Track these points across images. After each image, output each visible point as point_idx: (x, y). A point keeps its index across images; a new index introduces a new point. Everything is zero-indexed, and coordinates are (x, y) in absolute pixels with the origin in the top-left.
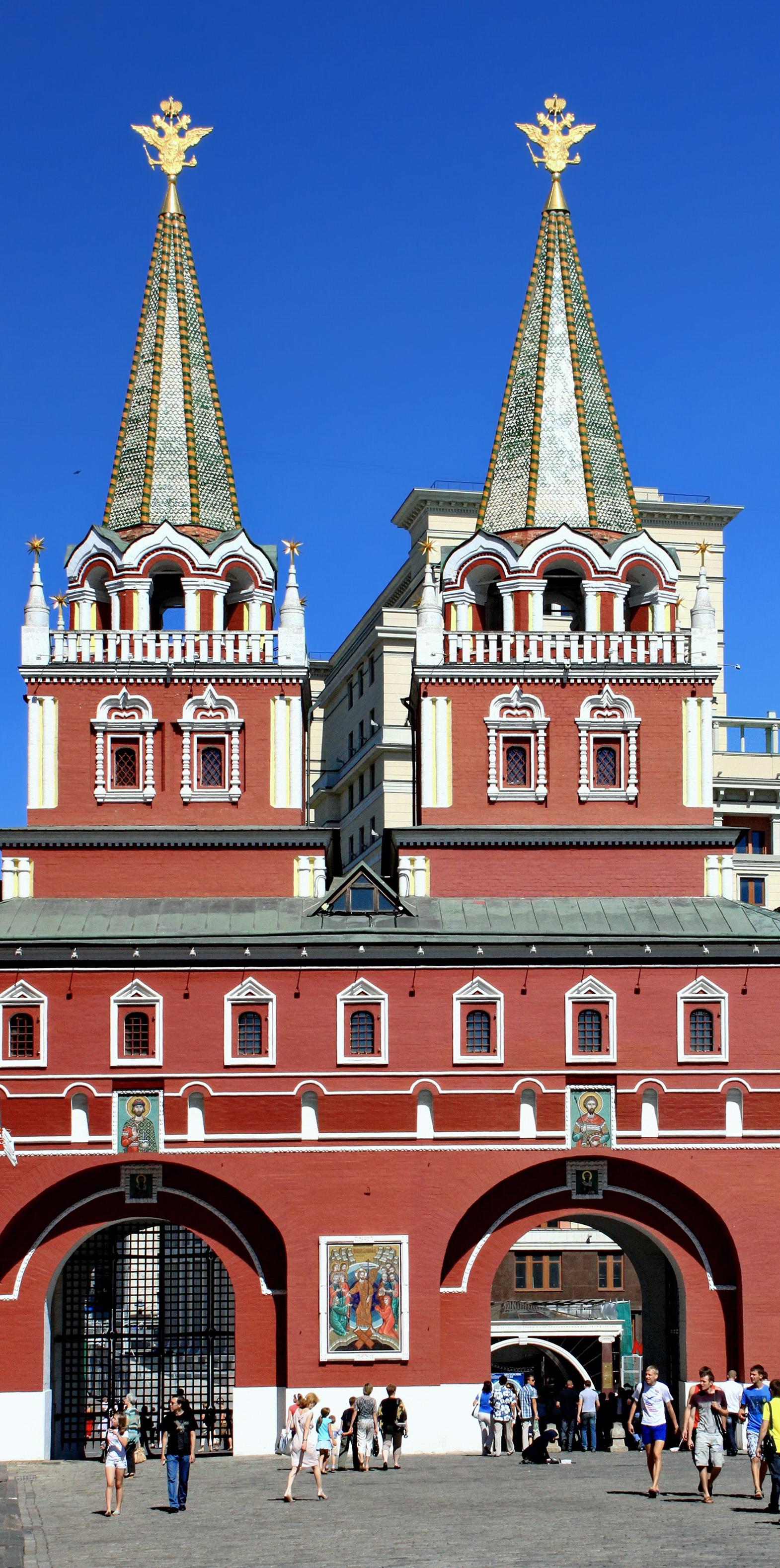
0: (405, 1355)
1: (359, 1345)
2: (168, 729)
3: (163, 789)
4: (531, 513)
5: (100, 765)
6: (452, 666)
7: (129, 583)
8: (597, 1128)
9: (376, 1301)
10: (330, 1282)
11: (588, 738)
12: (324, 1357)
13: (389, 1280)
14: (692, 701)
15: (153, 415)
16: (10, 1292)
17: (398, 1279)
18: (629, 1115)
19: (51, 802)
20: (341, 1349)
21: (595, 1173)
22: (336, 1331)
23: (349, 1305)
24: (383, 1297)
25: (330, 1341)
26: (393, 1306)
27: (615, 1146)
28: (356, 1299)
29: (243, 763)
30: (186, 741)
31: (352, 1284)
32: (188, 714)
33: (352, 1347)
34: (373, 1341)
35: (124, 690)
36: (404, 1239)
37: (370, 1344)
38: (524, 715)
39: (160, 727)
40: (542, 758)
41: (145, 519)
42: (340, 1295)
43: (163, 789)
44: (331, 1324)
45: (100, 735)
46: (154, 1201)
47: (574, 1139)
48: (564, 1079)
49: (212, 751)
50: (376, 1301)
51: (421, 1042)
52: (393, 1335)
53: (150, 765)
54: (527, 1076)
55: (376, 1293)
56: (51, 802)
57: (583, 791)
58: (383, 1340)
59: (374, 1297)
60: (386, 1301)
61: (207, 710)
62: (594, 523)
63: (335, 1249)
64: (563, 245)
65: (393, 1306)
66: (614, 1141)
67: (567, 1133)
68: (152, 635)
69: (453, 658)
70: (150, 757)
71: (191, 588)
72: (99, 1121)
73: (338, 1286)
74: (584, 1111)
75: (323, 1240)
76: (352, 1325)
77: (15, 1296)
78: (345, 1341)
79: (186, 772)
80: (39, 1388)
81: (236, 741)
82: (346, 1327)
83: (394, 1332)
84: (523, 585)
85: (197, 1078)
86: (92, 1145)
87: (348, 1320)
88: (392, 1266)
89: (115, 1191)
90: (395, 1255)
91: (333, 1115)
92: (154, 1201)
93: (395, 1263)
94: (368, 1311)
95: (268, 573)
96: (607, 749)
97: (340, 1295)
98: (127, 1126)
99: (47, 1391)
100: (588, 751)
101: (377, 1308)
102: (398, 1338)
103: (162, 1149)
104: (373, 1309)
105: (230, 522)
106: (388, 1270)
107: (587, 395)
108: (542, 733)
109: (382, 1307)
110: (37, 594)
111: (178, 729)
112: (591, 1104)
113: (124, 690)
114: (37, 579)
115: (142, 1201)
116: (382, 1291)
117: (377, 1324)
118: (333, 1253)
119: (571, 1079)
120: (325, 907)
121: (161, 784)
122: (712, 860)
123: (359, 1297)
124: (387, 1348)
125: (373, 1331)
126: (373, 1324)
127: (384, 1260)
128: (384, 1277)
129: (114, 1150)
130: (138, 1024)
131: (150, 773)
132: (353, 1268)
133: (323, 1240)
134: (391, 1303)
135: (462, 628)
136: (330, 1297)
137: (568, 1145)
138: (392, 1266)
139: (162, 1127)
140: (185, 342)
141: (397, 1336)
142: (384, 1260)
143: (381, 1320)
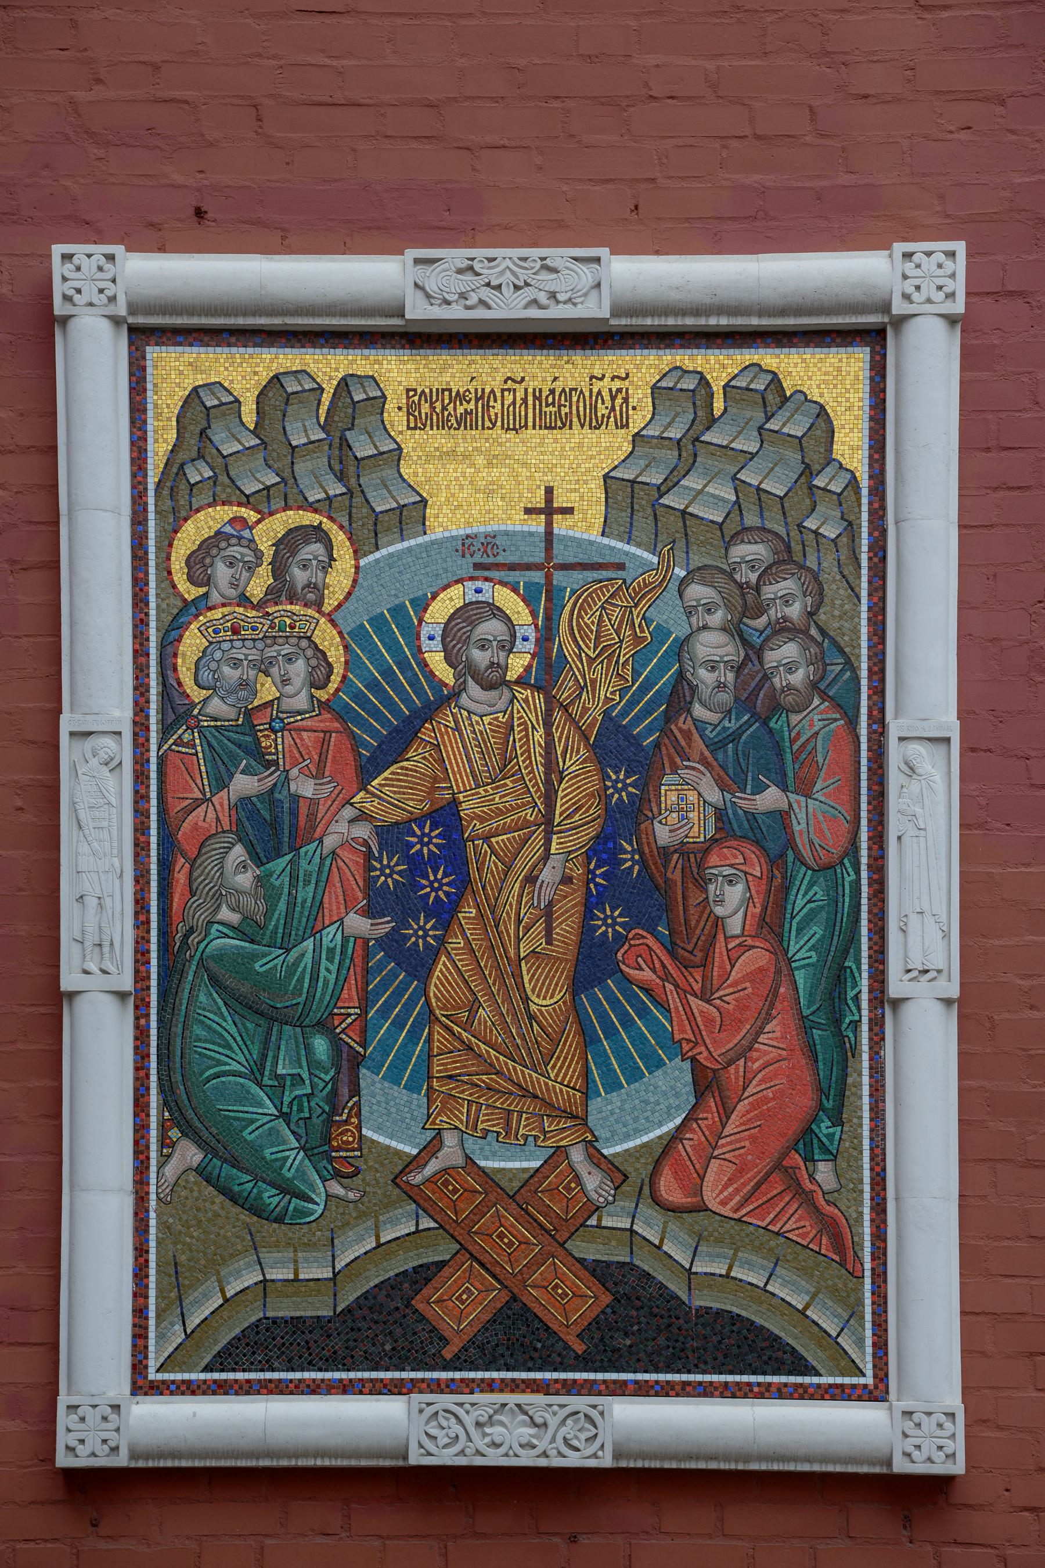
1: (460, 1307)
9: (637, 891)
12: (114, 1406)
13: (756, 696)
17: (855, 685)
20: (273, 1348)
23: (358, 924)
24: (694, 859)
26: (803, 948)
31: (389, 721)
34: (600, 1272)
37: (570, 1304)
42: (273, 829)
52: (797, 1224)
55: (623, 820)
58: (685, 1259)
59: (602, 848)
60: (732, 901)
65: (803, 948)
73: (245, 739)
76: (389, 1123)
82: (328, 1134)
83: (806, 1199)
87: (350, 1063)
88: (786, 558)
97: (273, 829)
101: (643, 963)
104: (592, 964)
106: (746, 602)
109: (693, 945)
116: (685, 805)
118: (202, 411)
123: (455, 856)
125: (593, 1181)
126: (601, 1110)
128: (713, 645)
133: (99, 280)
134: (771, 922)
138: (786, 558)
141: (837, 1237)
142: (707, 495)
143: (674, 1080)
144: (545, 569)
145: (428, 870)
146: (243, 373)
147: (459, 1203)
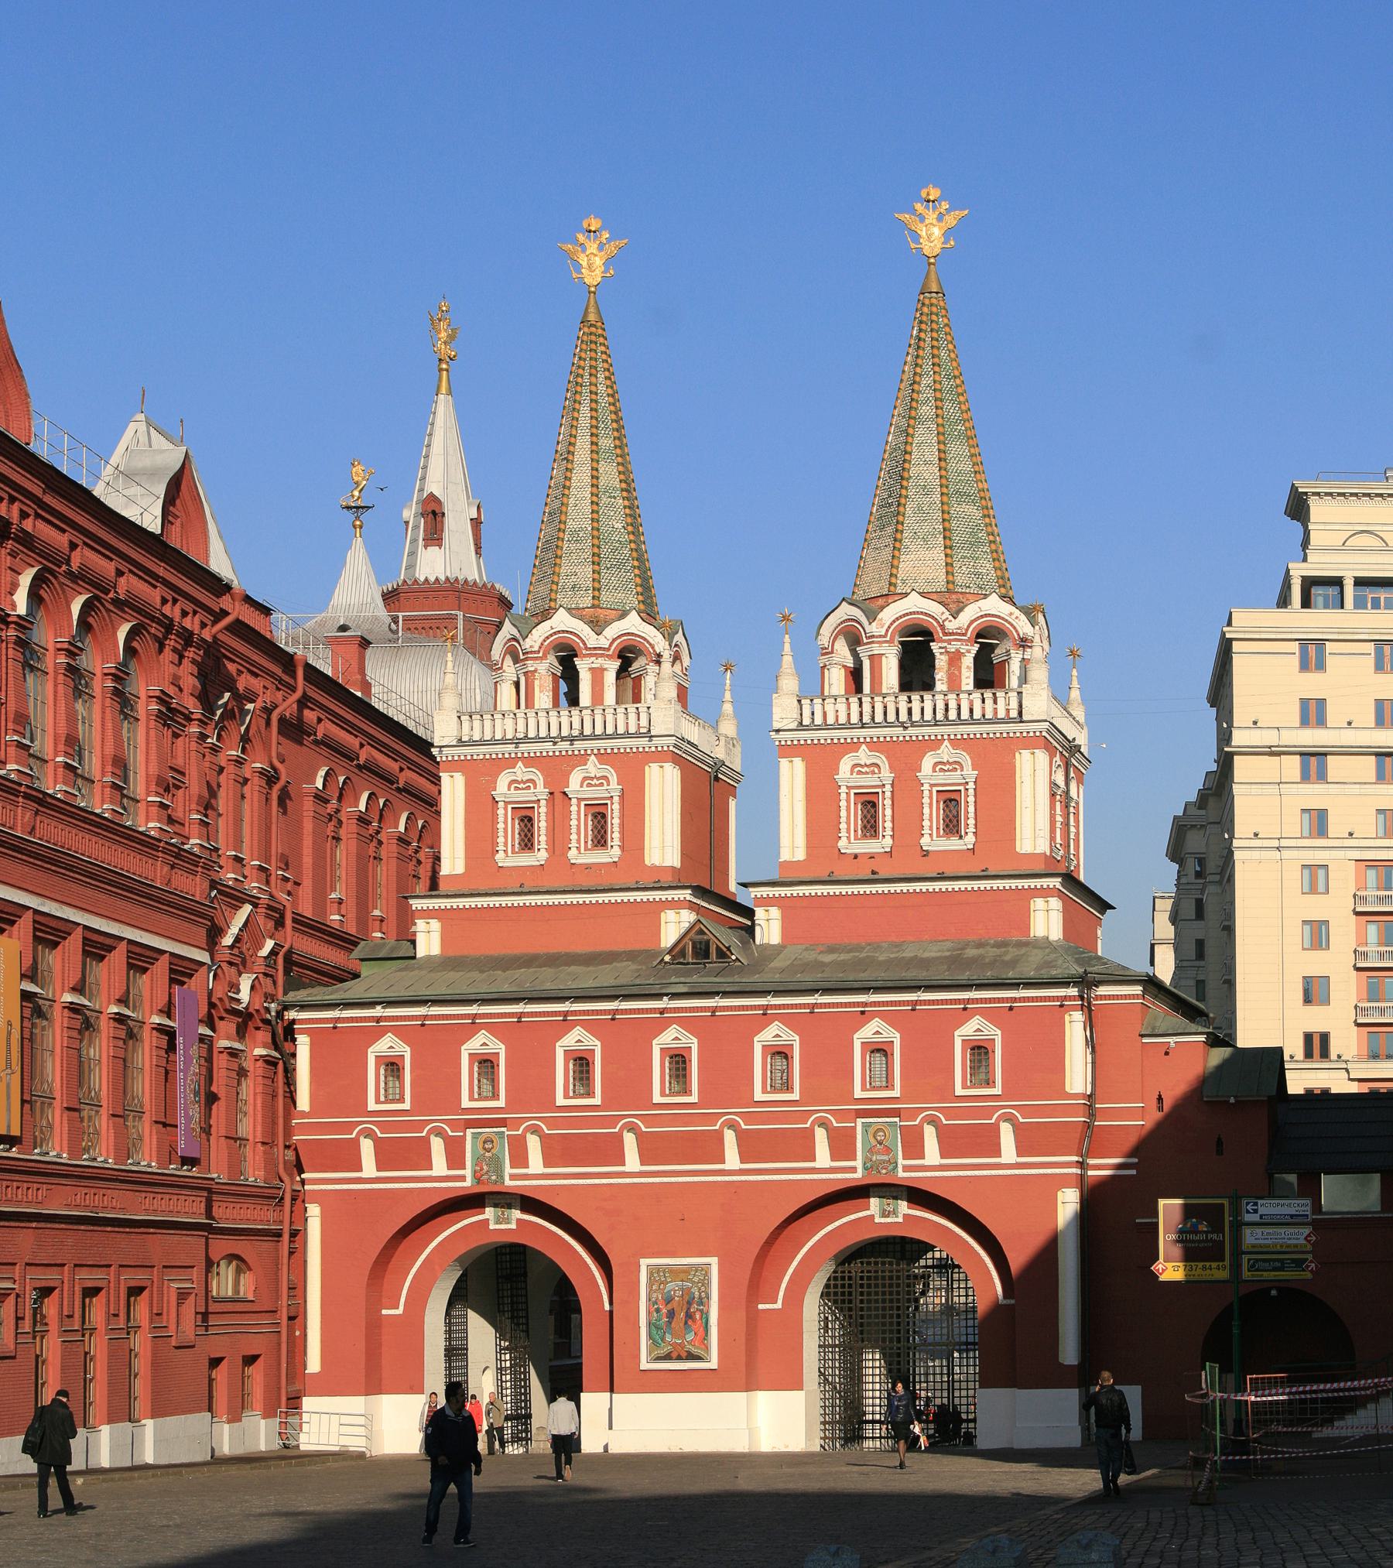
0: (713, 1364)
1: (674, 1355)
2: (558, 796)
4: (893, 580)
5: (501, 833)
6: (807, 728)
7: (531, 666)
8: (886, 1158)
9: (689, 1316)
10: (649, 1299)
11: (931, 792)
12: (644, 1365)
13: (700, 1298)
14: (1026, 753)
15: (564, 509)
18: (914, 1146)
19: (460, 869)
20: (659, 1359)
25: (649, 1352)
27: (901, 1174)
28: (671, 1314)
29: (622, 825)
30: (574, 808)
31: (669, 1300)
33: (667, 1357)
35: (520, 764)
36: (714, 1261)
37: (684, 1355)
38: (873, 773)
40: (888, 812)
41: (553, 604)
42: (658, 1311)
44: (650, 1336)
45: (501, 805)
46: (513, 1226)
47: (865, 1168)
50: (689, 1316)
54: (822, 1111)
56: (460, 869)
57: (925, 841)
58: (694, 1350)
61: (592, 779)
62: (951, 586)
63: (653, 1271)
64: (934, 326)
66: (900, 1169)
67: (858, 1163)
68: (553, 713)
69: (806, 721)
70: (543, 824)
71: (582, 665)
72: (455, 1158)
73: (656, 1303)
74: (873, 1142)
75: (644, 1262)
76: (668, 1338)
77: (400, 1311)
78: (662, 1352)
79: (574, 837)
81: (616, 807)
82: (663, 1339)
84: (876, 649)
85: (533, 1117)
89: (480, 1217)
90: (706, 1274)
92: (513, 1226)
93: (706, 1282)
96: (950, 801)
97: (658, 1311)
98: (478, 1161)
100: (931, 805)
101: (690, 1322)
102: (707, 1349)
103: (508, 1182)
105: (633, 600)
107: (952, 466)
109: (694, 1321)
112: (880, 1136)
113: (520, 764)
117: (690, 1337)
120: (667, 958)
121: (552, 848)
122: (1038, 903)
124: (698, 1358)
127: (696, 1279)
129: (468, 1183)
132: (670, 1286)
133: (644, 1262)
135: (834, 692)
136: (649, 1313)
137: (859, 1174)
139: (507, 1161)
140: (595, 439)
142: (696, 1279)
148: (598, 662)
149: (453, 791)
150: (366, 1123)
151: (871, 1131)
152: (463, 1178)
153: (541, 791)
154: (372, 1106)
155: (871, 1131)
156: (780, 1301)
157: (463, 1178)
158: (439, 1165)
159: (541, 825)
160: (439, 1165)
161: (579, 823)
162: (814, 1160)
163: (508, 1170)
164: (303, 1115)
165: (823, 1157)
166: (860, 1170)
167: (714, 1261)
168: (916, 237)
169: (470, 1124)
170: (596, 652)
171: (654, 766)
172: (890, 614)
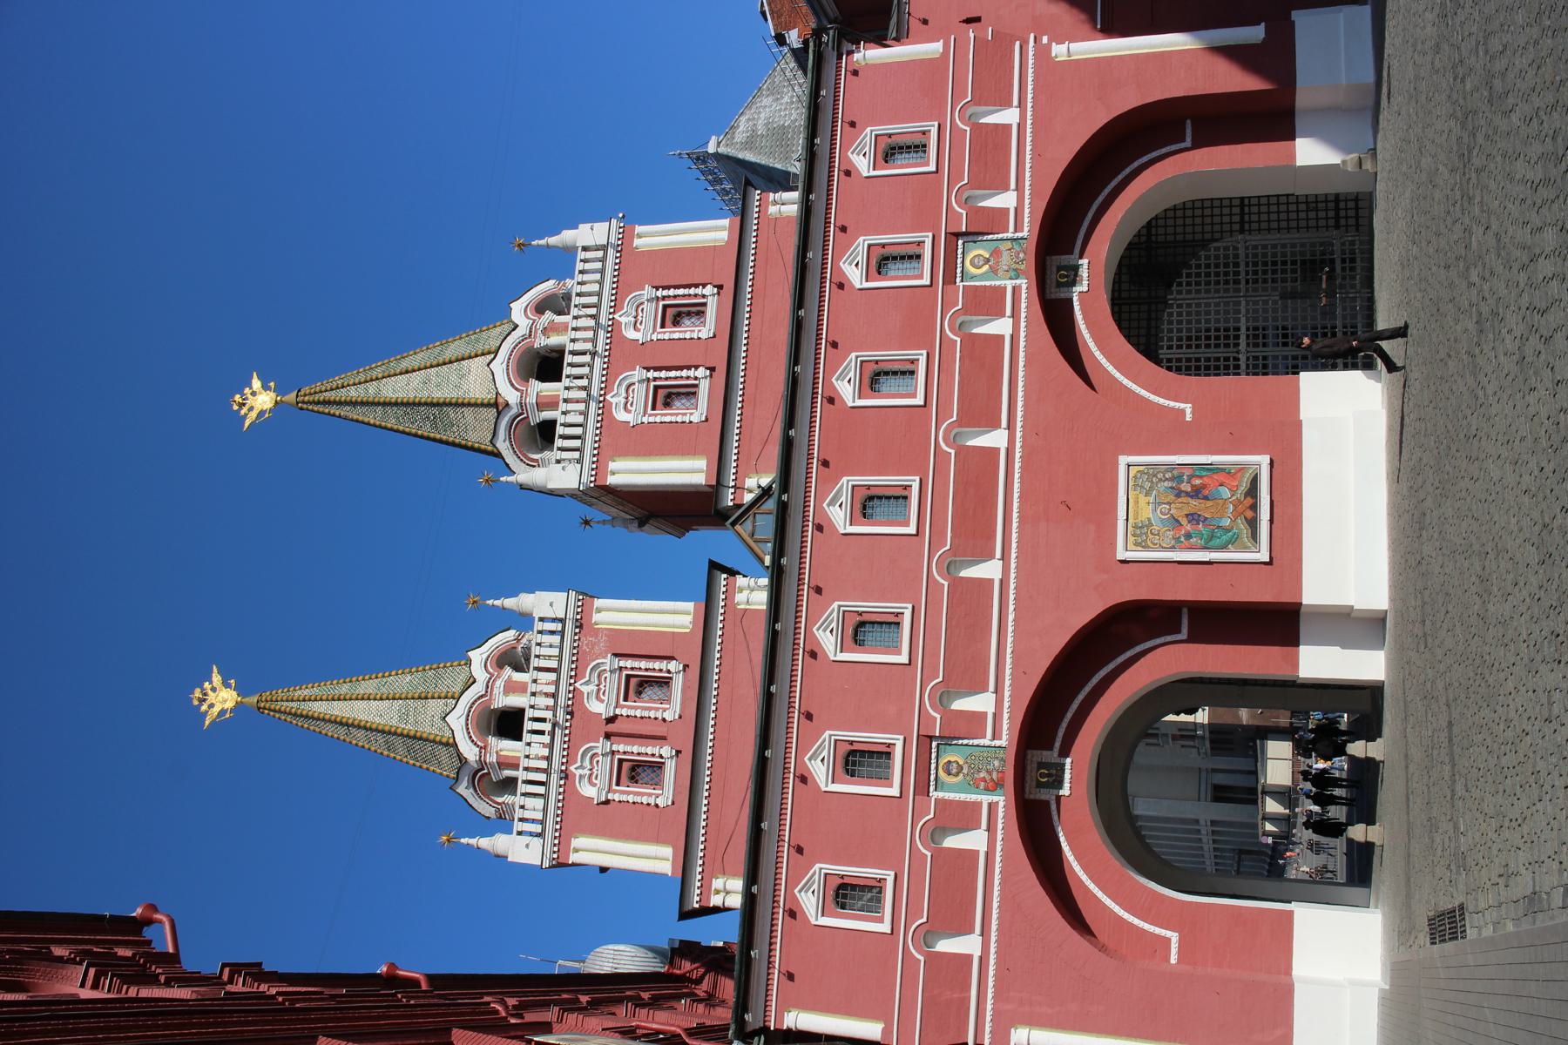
0: (1264, 460)
2: (611, 728)
3: (664, 738)
9: (1196, 493)
13: (1172, 479)
14: (637, 242)
16: (1169, 940)
17: (1171, 467)
20: (1254, 536)
21: (1059, 268)
22: (1232, 543)
25: (1245, 549)
28: (1194, 518)
32: (598, 708)
33: (1253, 524)
36: (1123, 460)
37: (1249, 501)
39: (608, 736)
40: (673, 374)
42: (1188, 536)
43: (664, 738)
44: (1223, 548)
45: (610, 796)
48: (949, 288)
49: (639, 686)
51: (903, 439)
53: (643, 750)
56: (667, 851)
58: (1244, 486)
60: (1198, 482)
67: (1009, 284)
70: (635, 749)
71: (503, 701)
72: (964, 817)
73: (1177, 539)
74: (986, 267)
76: (1226, 522)
77: (1174, 937)
80: (1291, 913)
81: (629, 663)
82: (1228, 530)
84: (532, 399)
86: (991, 828)
91: (975, 542)
94: (1209, 503)
95: (510, 634)
97: (1188, 536)
98: (974, 785)
99: (1293, 906)
101: (1206, 492)
102: (1242, 468)
104: (1206, 498)
108: (651, 374)
109: (1204, 486)
110: (484, 842)
111: (611, 720)
114: (473, 841)
115: (1067, 776)
116: (1186, 487)
117: (1225, 492)
118: (1136, 544)
119: (950, 278)
124: (1255, 481)
130: (855, 761)
131: (649, 750)
136: (1192, 548)
137: (1023, 283)
144: (1157, 504)
145: (1194, 518)
146: (1131, 539)
147: (1236, 513)
148: (500, 684)
149: (590, 850)
150: (906, 940)
151: (973, 270)
152: (992, 807)
153: (601, 746)
154: (885, 927)
155: (973, 270)
156: (1182, 406)
157: (992, 807)
158: (974, 840)
159: (635, 749)
160: (974, 840)
161: (642, 708)
162: (1002, 337)
163: (986, 742)
164: (887, 1031)
165: (1000, 327)
166: (1018, 282)
167: (1123, 460)
168: (262, 413)
169: (922, 789)
170: (489, 686)
171: (596, 617)
172: (511, 396)
